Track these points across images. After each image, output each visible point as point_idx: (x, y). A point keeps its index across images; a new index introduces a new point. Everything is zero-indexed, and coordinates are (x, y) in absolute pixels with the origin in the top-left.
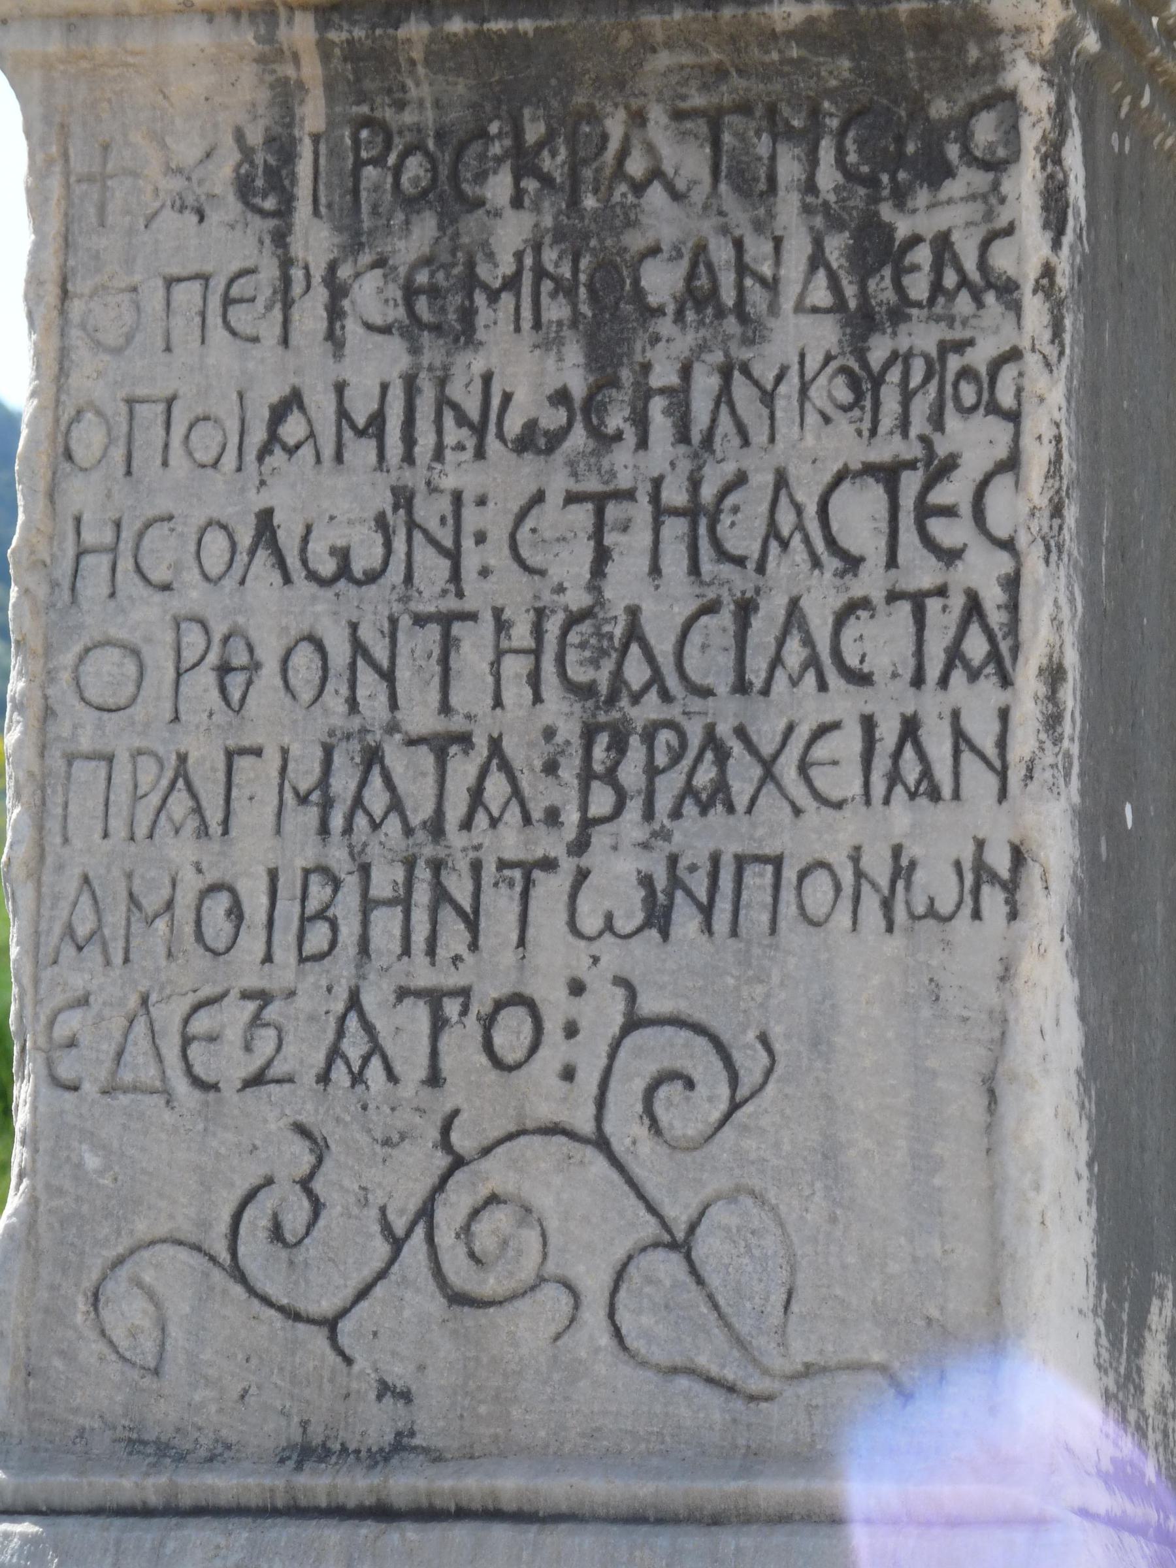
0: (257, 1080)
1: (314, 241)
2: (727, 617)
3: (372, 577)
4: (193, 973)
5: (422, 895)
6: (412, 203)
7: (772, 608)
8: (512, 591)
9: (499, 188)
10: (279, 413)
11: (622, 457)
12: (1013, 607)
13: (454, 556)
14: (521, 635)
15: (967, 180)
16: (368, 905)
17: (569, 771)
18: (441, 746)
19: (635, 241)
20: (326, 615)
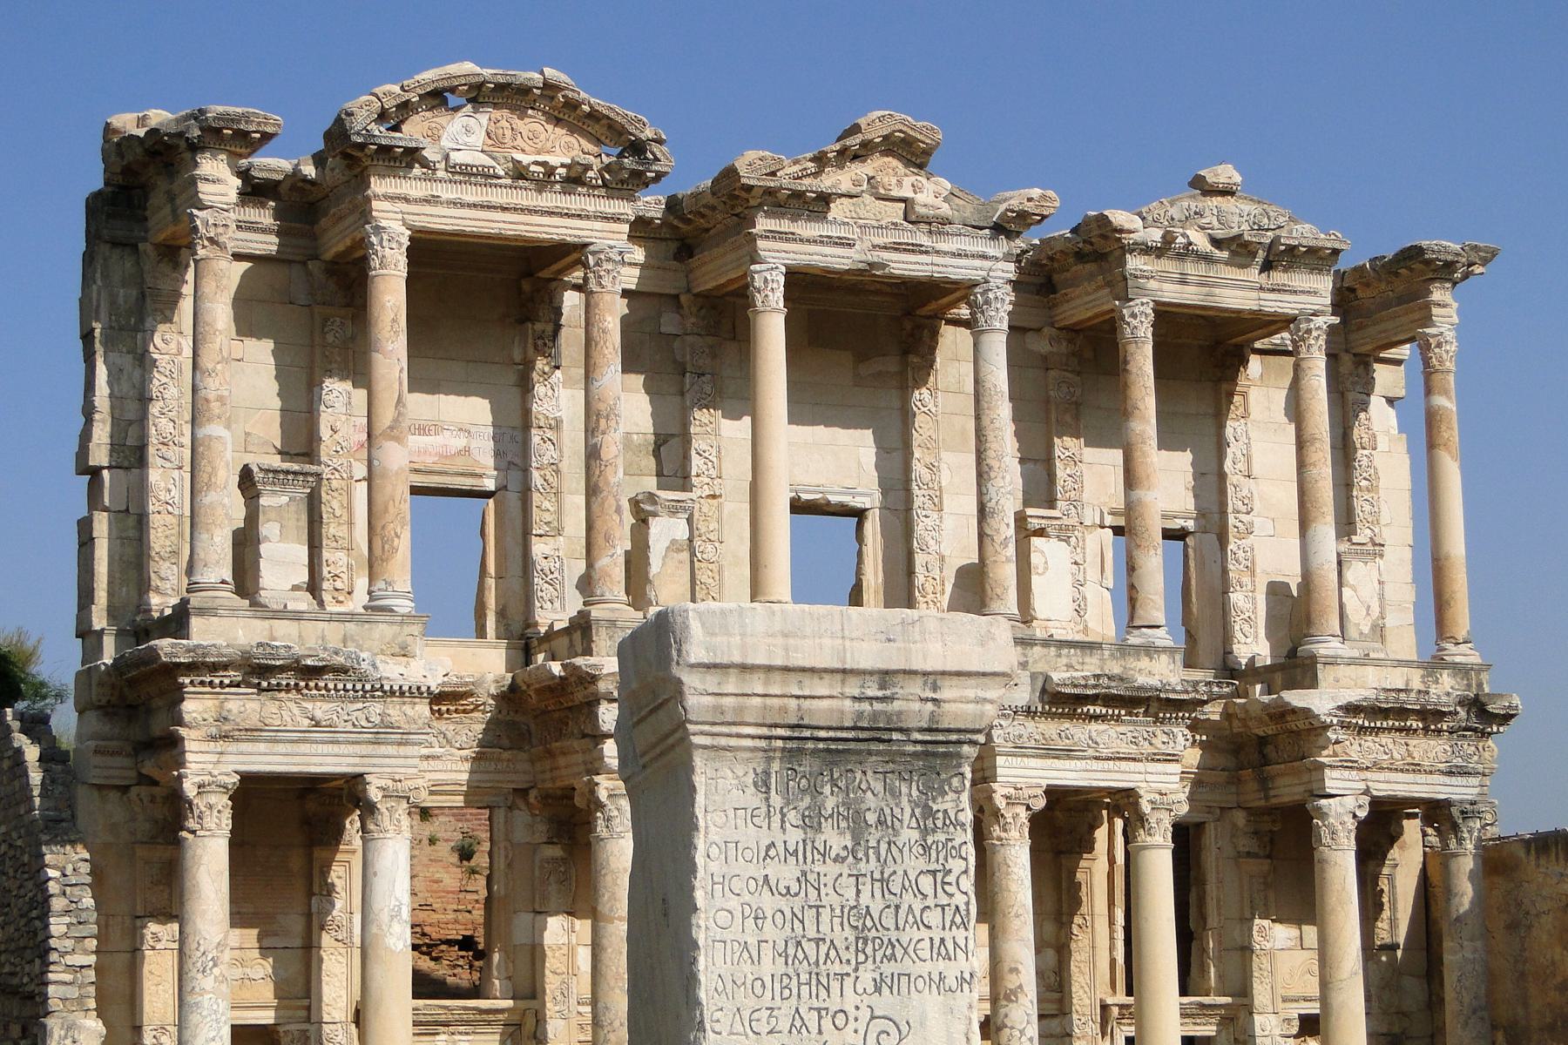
0: (770, 1032)
1: (777, 801)
2: (892, 909)
3: (796, 895)
4: (752, 1003)
5: (814, 982)
6: (804, 791)
7: (904, 907)
8: (834, 899)
9: (827, 789)
10: (768, 848)
11: (862, 864)
12: (968, 910)
13: (818, 890)
14: (838, 912)
15: (951, 796)
16: (799, 984)
17: (852, 949)
18: (818, 941)
19: (864, 806)
20: (783, 903)
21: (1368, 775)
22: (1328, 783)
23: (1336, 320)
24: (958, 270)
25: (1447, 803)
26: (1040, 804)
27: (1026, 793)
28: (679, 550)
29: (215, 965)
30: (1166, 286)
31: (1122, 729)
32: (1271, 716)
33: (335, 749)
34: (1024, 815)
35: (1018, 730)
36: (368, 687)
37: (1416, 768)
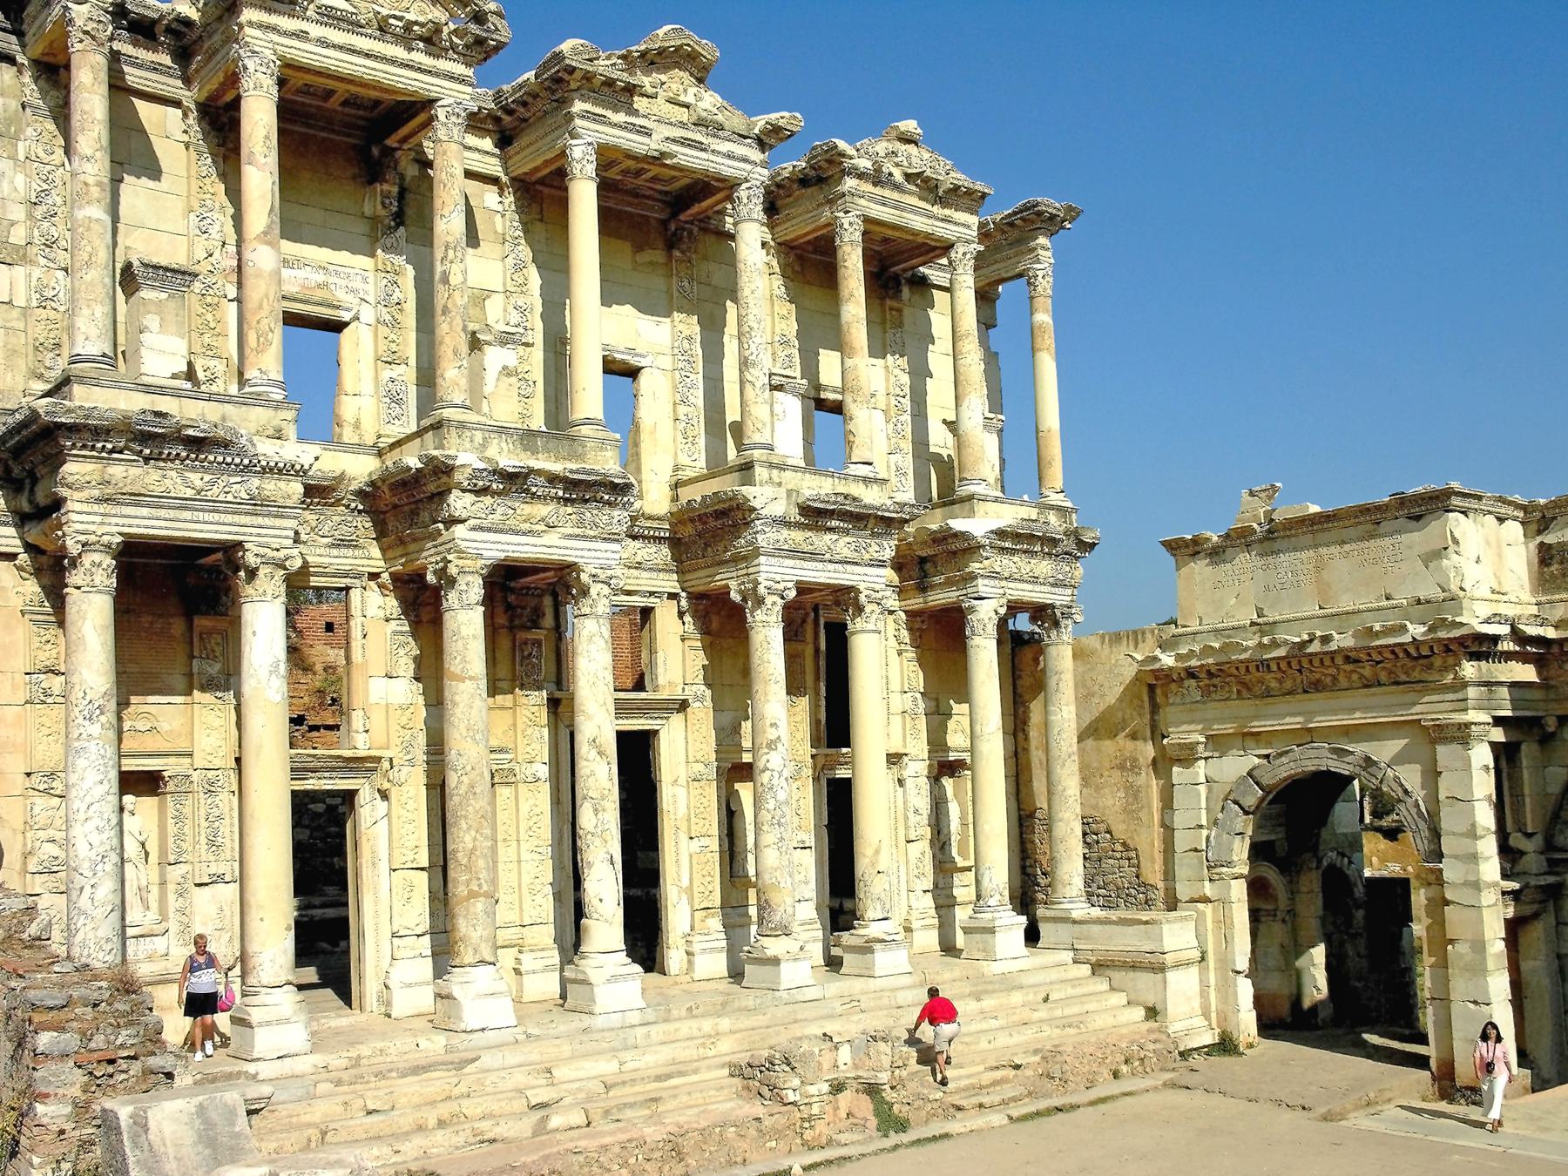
21: (1004, 583)
22: (981, 588)
23: (982, 248)
24: (728, 169)
25: (1052, 606)
26: (792, 594)
27: (781, 586)
28: (509, 375)
29: (102, 713)
30: (872, 205)
31: (848, 539)
32: (934, 541)
33: (217, 516)
34: (780, 602)
35: (775, 536)
36: (246, 462)
37: (1035, 580)
